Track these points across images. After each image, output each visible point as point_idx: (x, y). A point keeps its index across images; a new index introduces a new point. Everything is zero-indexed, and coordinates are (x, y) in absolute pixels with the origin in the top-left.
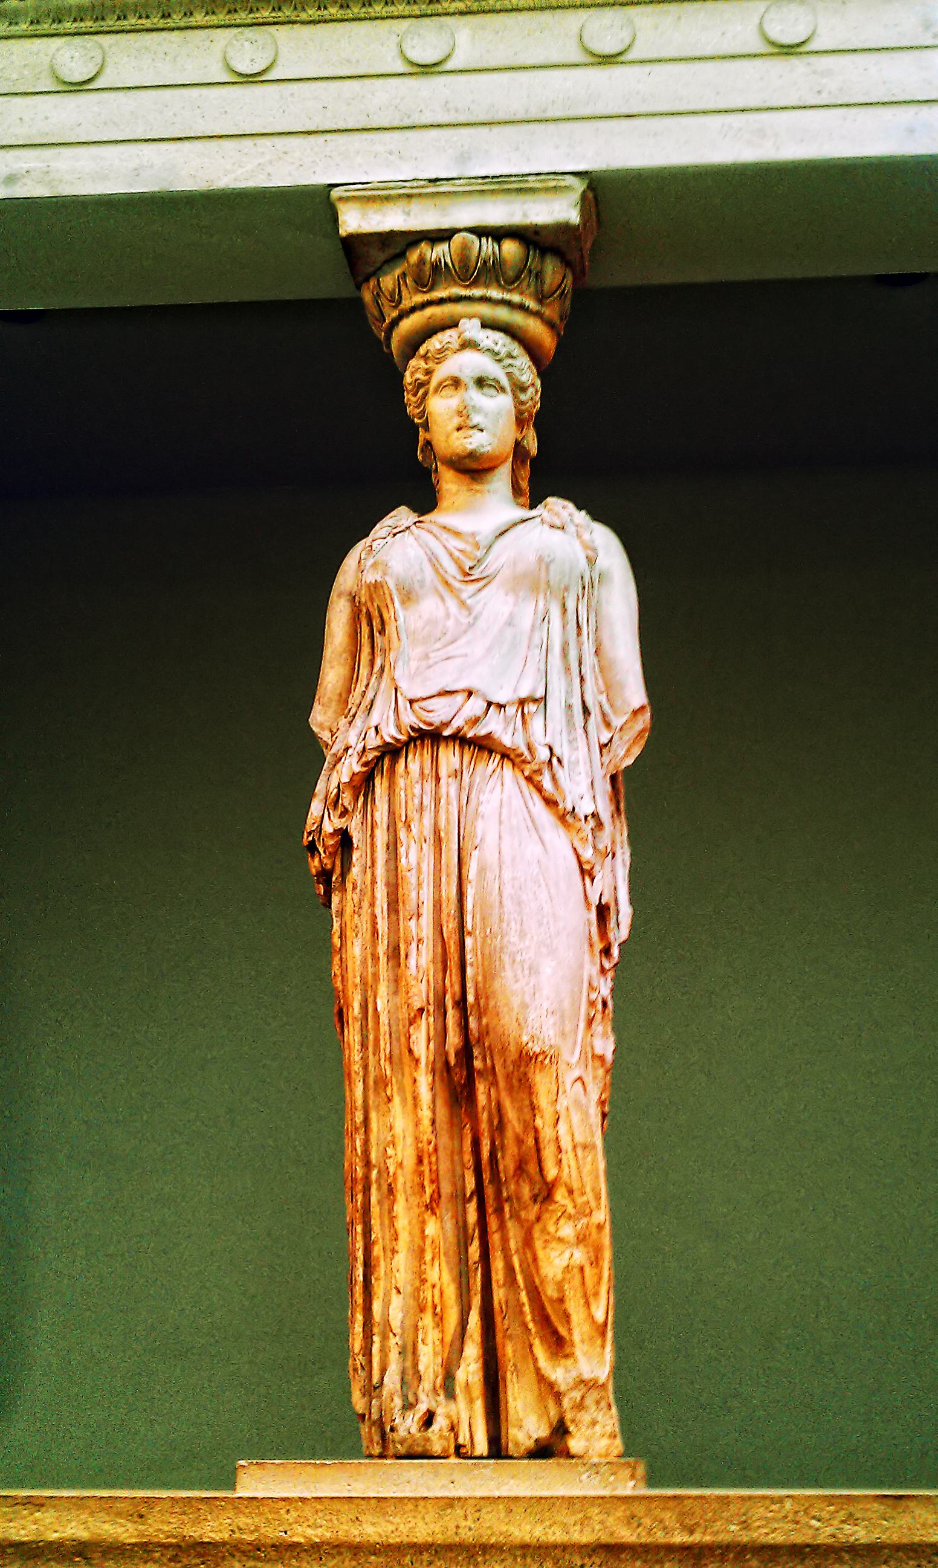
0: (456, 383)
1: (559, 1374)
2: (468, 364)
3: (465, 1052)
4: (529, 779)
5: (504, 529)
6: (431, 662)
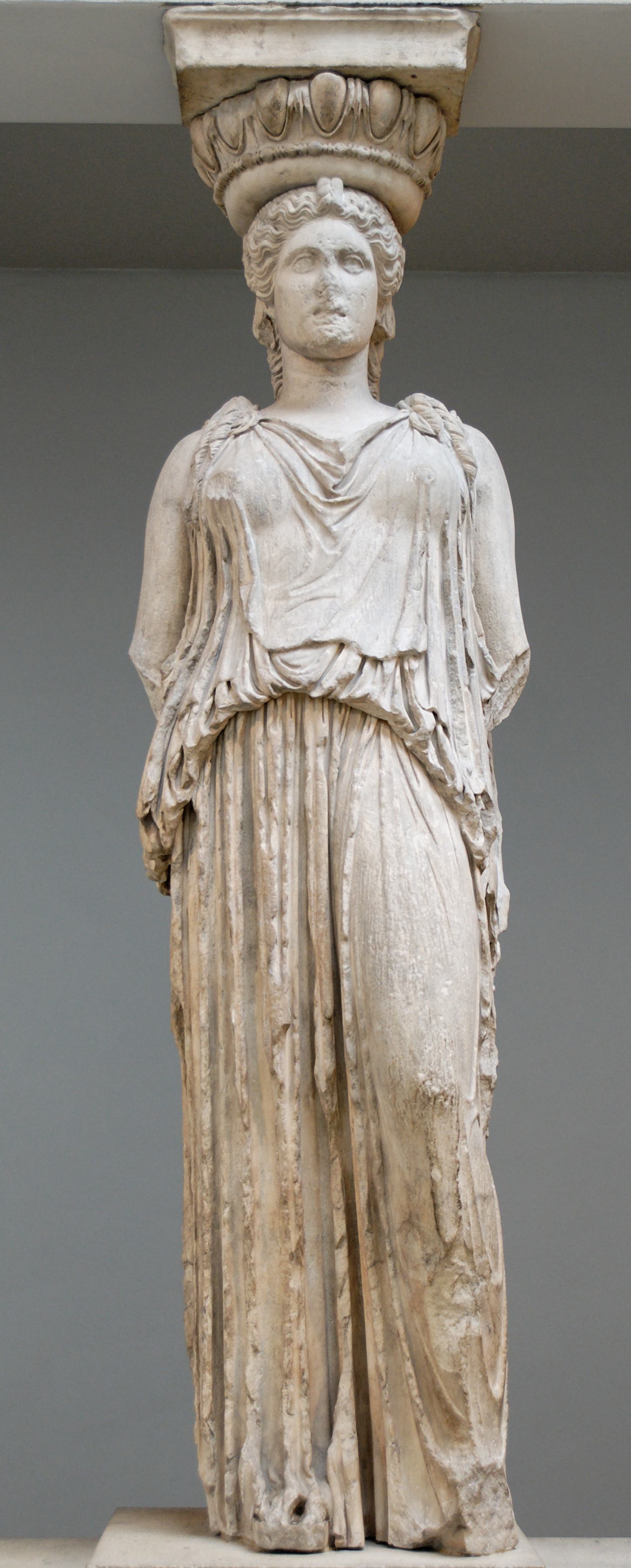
0: (313, 255)
1: (457, 1463)
2: (333, 233)
3: (339, 1076)
4: (409, 751)
5: (369, 437)
6: (291, 602)
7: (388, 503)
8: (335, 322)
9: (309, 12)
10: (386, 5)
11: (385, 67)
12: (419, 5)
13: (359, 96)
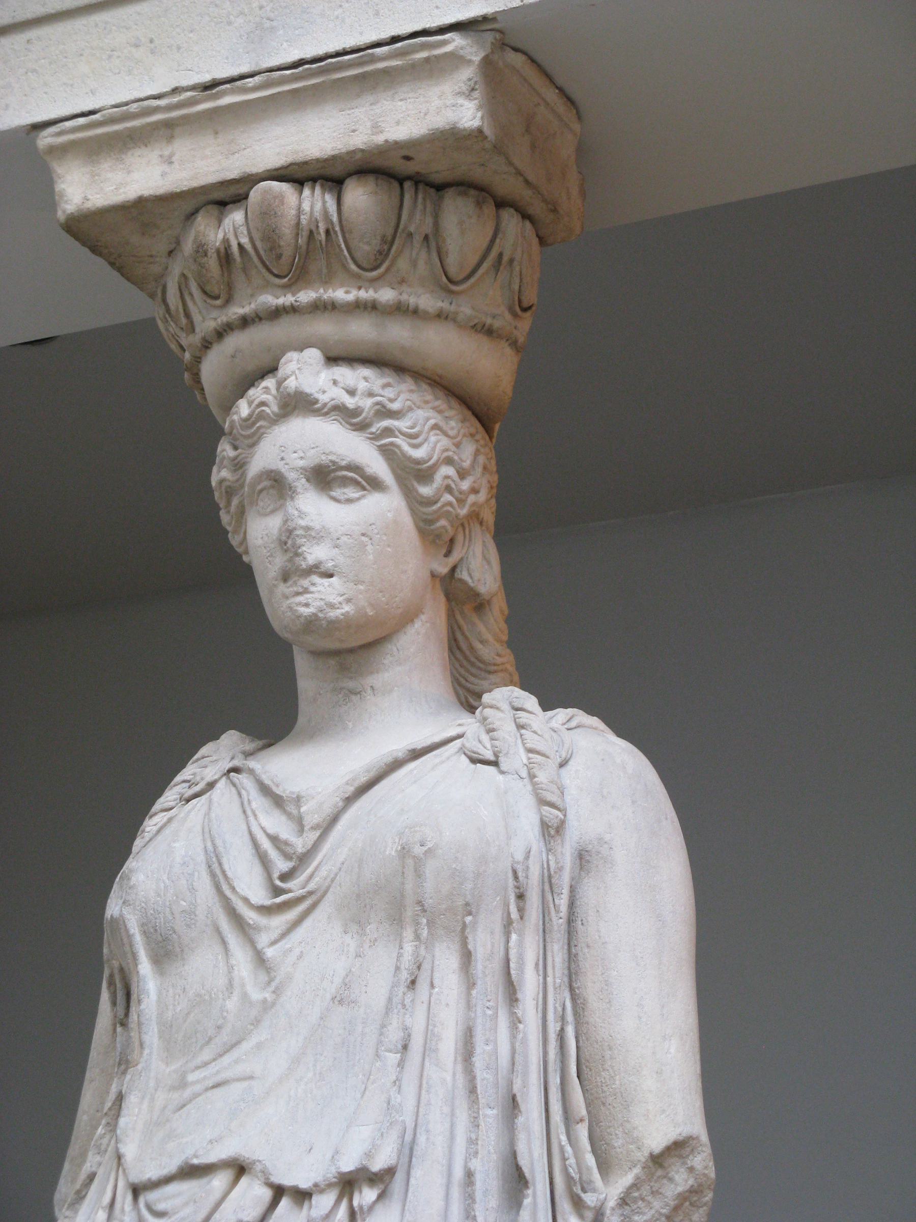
5: (363, 779)
7: (358, 896)
8: (312, 589)
9: (233, 92)
10: (345, 53)
12: (395, 40)
13: (318, 206)
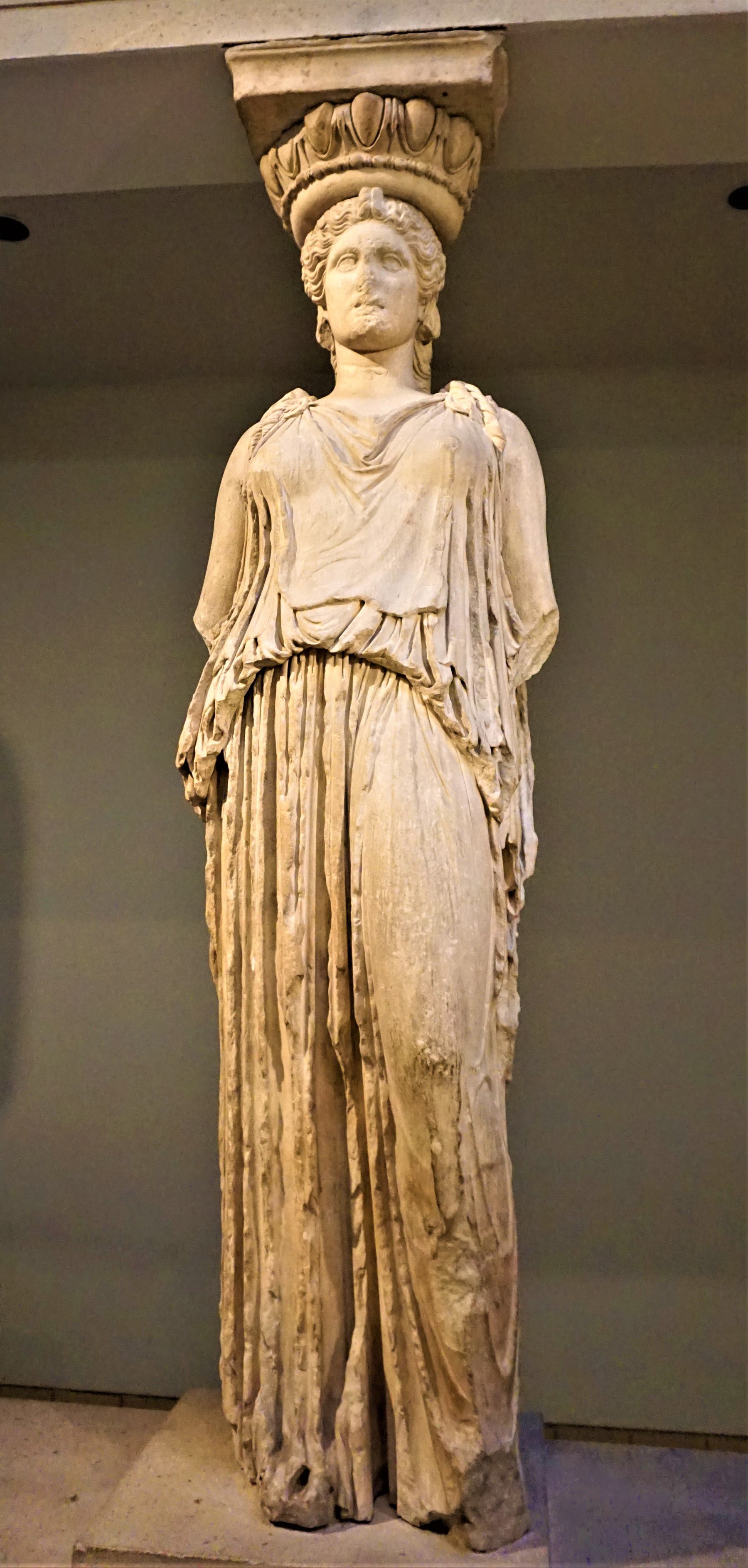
3: (352, 1030)
4: (429, 705)
11: (417, 85)
12: (449, 29)
